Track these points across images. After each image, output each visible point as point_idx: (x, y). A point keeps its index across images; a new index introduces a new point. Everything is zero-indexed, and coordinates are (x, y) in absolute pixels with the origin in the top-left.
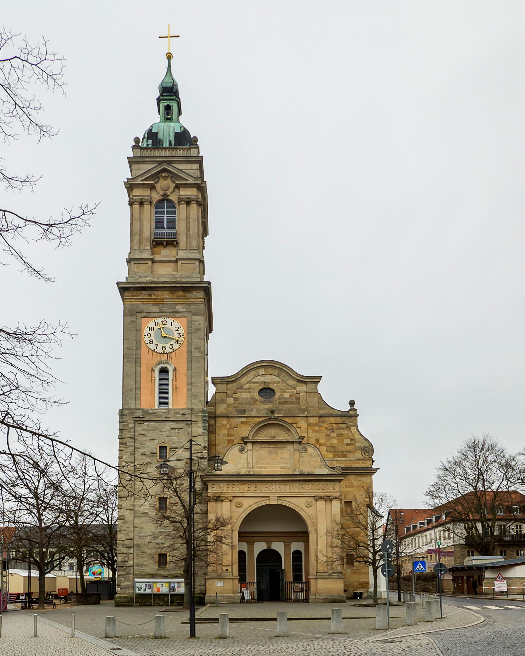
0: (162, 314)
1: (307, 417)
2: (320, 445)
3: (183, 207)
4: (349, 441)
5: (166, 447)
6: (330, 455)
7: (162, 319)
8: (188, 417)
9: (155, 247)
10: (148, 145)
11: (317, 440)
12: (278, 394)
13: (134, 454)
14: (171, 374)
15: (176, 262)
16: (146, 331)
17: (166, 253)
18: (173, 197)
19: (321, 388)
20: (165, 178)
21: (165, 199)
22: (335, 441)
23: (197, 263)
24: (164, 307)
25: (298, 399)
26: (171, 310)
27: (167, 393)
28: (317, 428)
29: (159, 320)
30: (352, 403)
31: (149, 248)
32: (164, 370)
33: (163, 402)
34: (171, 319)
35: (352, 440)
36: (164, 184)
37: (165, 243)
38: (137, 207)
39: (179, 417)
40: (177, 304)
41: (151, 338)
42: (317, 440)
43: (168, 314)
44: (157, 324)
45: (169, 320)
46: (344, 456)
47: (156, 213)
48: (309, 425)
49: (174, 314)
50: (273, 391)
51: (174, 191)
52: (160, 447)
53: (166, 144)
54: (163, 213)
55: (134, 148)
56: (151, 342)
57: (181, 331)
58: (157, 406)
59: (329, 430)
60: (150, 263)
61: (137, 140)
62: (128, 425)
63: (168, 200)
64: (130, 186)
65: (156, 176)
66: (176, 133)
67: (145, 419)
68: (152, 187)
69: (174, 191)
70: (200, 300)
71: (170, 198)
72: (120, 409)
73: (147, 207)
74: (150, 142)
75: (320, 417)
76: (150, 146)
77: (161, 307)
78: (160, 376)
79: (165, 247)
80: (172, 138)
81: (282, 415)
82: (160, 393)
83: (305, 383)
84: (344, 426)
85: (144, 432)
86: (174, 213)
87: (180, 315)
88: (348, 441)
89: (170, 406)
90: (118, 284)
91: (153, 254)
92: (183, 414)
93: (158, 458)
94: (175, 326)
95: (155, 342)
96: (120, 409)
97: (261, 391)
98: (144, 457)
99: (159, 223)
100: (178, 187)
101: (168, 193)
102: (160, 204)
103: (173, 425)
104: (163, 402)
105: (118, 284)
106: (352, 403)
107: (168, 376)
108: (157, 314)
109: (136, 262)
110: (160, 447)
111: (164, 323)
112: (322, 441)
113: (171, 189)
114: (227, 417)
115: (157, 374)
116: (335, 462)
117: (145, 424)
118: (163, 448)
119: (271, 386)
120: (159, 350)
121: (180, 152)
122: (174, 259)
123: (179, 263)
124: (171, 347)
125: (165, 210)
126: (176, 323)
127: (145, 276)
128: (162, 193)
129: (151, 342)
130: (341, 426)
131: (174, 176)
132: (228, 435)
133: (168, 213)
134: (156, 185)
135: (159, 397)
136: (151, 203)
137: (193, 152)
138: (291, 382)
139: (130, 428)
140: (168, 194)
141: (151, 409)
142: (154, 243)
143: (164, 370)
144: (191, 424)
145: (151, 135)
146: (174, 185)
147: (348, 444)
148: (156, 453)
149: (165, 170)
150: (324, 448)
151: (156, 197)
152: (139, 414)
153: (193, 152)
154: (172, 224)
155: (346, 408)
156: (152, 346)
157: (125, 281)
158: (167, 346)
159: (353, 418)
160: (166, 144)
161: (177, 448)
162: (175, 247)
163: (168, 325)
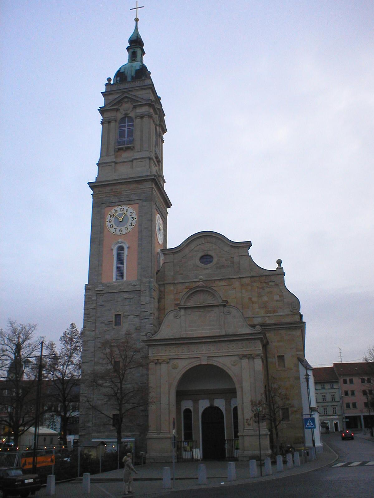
0: (121, 203)
1: (240, 278)
2: (253, 303)
3: (139, 120)
4: (276, 297)
5: (120, 315)
6: (262, 313)
7: (120, 207)
8: (138, 288)
9: (117, 152)
10: (117, 81)
11: (250, 299)
12: (215, 260)
13: (95, 323)
14: (126, 251)
15: (132, 161)
16: (108, 218)
17: (125, 155)
18: (132, 115)
19: (251, 252)
20: (127, 102)
21: (126, 116)
22: (265, 299)
23: (147, 160)
24: (122, 198)
25: (233, 262)
26: (127, 199)
27: (123, 267)
28: (249, 288)
29: (118, 208)
30: (279, 262)
31: (113, 153)
33: (120, 276)
34: (127, 206)
35: (280, 296)
36: (127, 106)
37: (124, 149)
38: (106, 125)
39: (132, 288)
40: (131, 194)
41: (111, 224)
42: (250, 299)
43: (125, 202)
45: (125, 207)
46: (275, 312)
47: (120, 127)
48: (242, 285)
49: (129, 202)
50: (211, 257)
51: (132, 110)
52: (116, 315)
53: (129, 79)
54: (125, 126)
55: (106, 85)
56: (111, 226)
58: (114, 280)
59: (260, 288)
60: (113, 164)
61: (109, 79)
62: (91, 298)
63: (128, 117)
64: (102, 111)
65: (119, 102)
66: (136, 70)
67: (103, 292)
68: (117, 110)
69: (132, 110)
70: (149, 189)
71: (130, 115)
72: (86, 285)
73: (113, 124)
74: (118, 78)
75: (252, 277)
76: (118, 81)
77: (119, 198)
78: (118, 254)
79: (125, 151)
80: (133, 74)
81: (219, 278)
82: (117, 268)
83: (237, 247)
84: (273, 284)
85: (103, 303)
86: (133, 125)
87: (133, 202)
88: (276, 297)
89: (125, 279)
90: (89, 183)
91: (116, 157)
92: (134, 286)
93: (113, 325)
94: (130, 212)
95: (115, 226)
96: (86, 285)
97: (202, 258)
98: (103, 325)
99: (122, 134)
100: (135, 107)
101: (128, 112)
102: (123, 120)
103: (126, 296)
104: (120, 276)
105: (89, 183)
106: (279, 262)
107: (123, 253)
108: (117, 204)
109: (102, 165)
110: (116, 315)
111: (121, 210)
112: (255, 299)
113: (131, 109)
114: (174, 283)
115: (115, 252)
116: (267, 318)
117: (105, 295)
118: (118, 316)
119: (210, 253)
120: (118, 232)
121: (138, 83)
122: (131, 160)
123: (135, 161)
124: (126, 229)
125: (126, 124)
126: (131, 210)
127: (111, 176)
128: (124, 113)
129: (111, 226)
130: (270, 284)
131: (132, 100)
132: (176, 300)
133: (128, 126)
134: (120, 108)
135: (117, 271)
136: (116, 121)
137: (147, 82)
138: (227, 249)
139: (93, 301)
140: (128, 113)
141: (109, 283)
142: (117, 149)
143: (121, 249)
144: (140, 294)
145: (120, 75)
146: (133, 106)
147: (277, 301)
148: (112, 321)
150: (256, 306)
151: (120, 116)
152: (100, 288)
153: (147, 82)
154: (131, 133)
155: (273, 267)
156: (112, 230)
157: (95, 181)
158: (123, 228)
159: (280, 276)
160: (129, 79)
161: (129, 316)
162: (132, 150)
163: (125, 210)
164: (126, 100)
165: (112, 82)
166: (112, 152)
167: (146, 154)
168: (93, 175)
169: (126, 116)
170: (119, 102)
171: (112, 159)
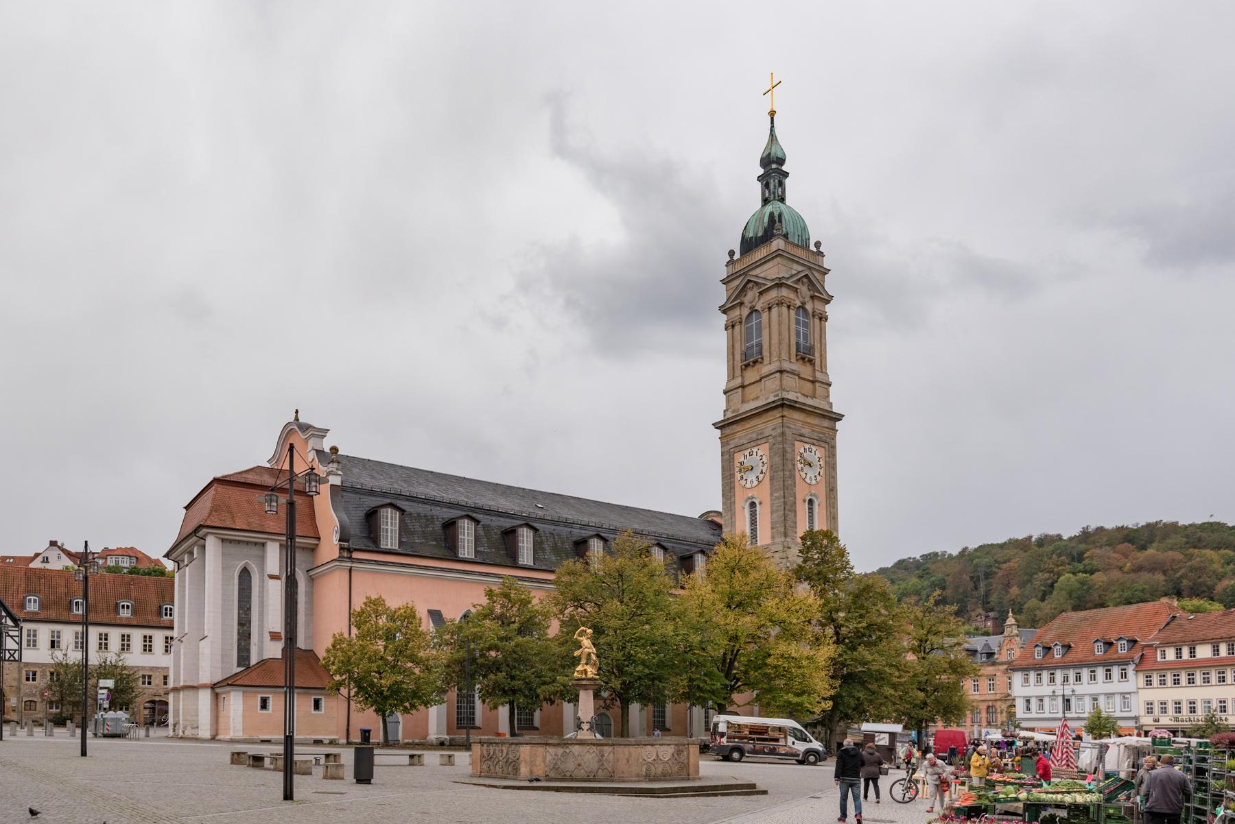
17: (751, 375)
18: (758, 307)
21: (753, 310)
29: (747, 453)
32: (753, 505)
36: (751, 295)
44: (745, 457)
57: (765, 459)
68: (741, 304)
73: (737, 328)
100: (761, 293)
143: (753, 505)
149: (749, 281)
151: (746, 312)
164: (750, 285)
165: (737, 256)
166: (738, 372)
167: (774, 367)
168: (717, 409)
169: (753, 310)
170: (743, 290)
171: (738, 381)
